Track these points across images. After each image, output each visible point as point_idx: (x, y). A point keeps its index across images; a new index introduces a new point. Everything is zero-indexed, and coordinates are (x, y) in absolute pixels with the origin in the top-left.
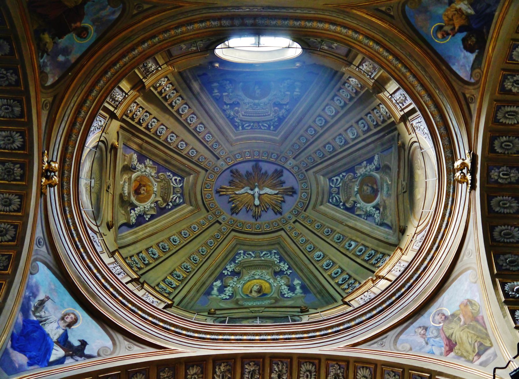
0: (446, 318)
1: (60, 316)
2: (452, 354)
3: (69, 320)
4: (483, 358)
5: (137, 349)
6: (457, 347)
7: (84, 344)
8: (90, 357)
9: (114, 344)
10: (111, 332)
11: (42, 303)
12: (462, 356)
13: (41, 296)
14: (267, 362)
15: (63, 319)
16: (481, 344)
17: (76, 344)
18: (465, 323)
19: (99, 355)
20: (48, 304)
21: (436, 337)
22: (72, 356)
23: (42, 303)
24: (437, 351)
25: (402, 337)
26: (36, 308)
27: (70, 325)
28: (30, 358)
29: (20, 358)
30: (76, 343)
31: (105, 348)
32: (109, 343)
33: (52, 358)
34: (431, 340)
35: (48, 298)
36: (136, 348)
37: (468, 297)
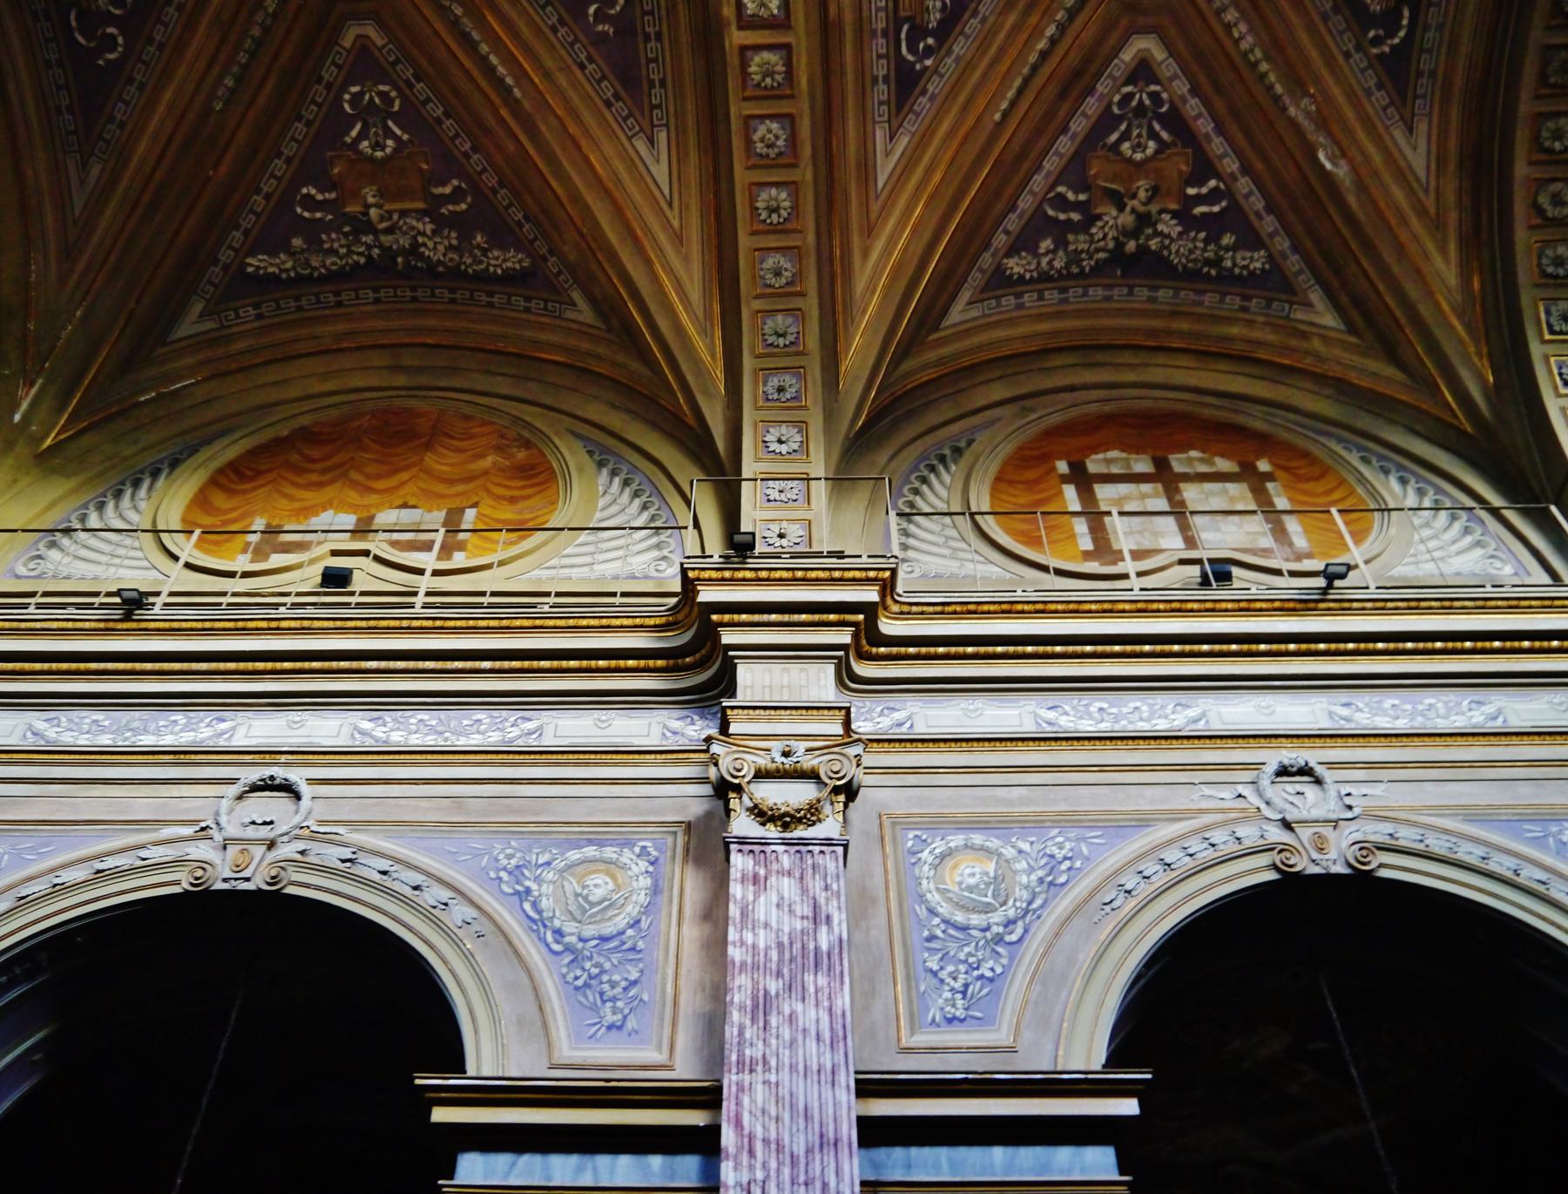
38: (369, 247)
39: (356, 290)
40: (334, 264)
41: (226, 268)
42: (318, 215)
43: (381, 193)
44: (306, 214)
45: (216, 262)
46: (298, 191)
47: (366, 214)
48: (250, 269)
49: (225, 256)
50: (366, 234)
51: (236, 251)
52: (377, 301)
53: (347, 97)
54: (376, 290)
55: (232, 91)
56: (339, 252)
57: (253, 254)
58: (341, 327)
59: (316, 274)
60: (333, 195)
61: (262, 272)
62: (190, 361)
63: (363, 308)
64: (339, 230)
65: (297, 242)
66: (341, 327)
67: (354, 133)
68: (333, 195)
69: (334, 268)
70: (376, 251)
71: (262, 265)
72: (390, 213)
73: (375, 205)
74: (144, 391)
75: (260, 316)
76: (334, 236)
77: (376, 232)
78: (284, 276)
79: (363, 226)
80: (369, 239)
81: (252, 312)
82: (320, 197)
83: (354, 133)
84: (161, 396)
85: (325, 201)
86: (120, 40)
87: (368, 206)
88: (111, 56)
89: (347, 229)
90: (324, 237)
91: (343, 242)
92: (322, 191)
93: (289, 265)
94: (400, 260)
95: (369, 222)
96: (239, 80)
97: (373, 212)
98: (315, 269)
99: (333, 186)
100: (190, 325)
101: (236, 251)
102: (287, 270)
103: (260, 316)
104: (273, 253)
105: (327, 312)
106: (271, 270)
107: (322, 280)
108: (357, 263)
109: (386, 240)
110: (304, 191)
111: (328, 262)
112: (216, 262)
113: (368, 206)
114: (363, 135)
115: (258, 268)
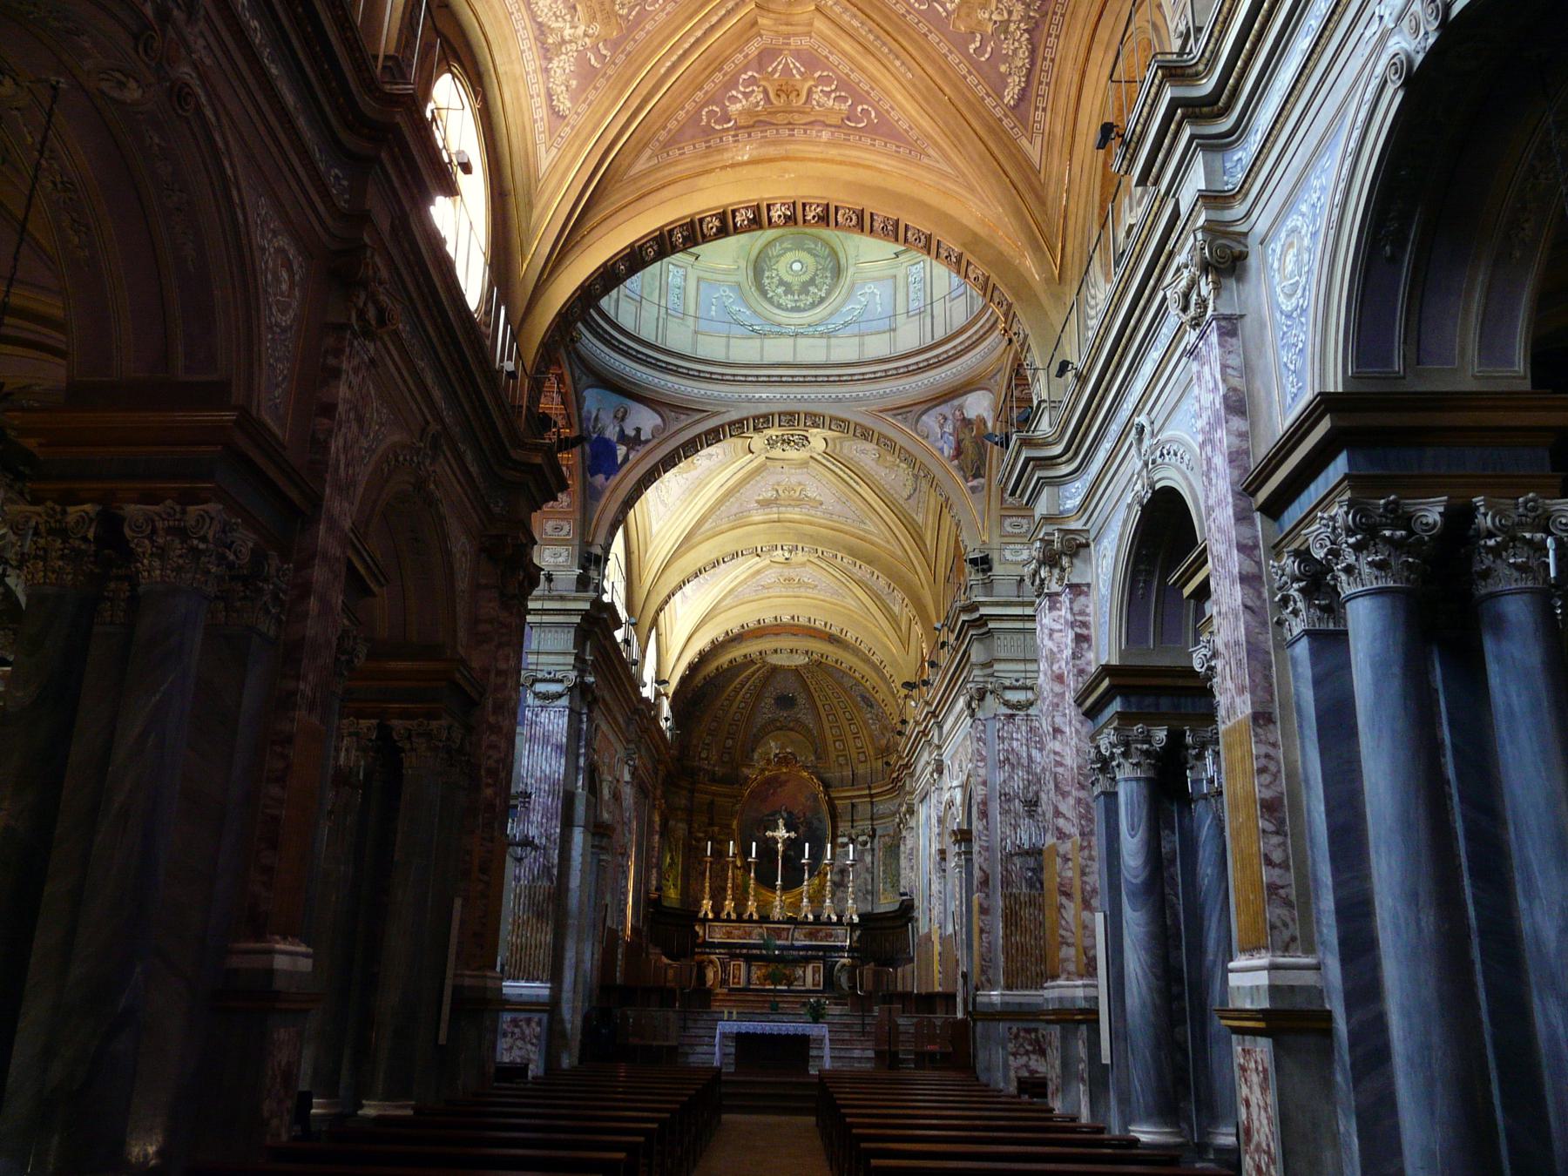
0: (964, 418)
1: (612, 416)
2: (956, 462)
3: (620, 415)
4: (975, 483)
5: (685, 420)
6: (962, 456)
7: (638, 430)
8: (647, 441)
9: (663, 420)
10: (658, 408)
11: (597, 418)
12: (962, 469)
13: (594, 416)
14: (803, 416)
15: (615, 417)
16: (978, 468)
17: (631, 433)
18: (975, 437)
19: (653, 437)
20: (602, 415)
21: (950, 434)
22: (633, 448)
23: (597, 418)
24: (946, 454)
25: (924, 418)
26: (594, 428)
27: (623, 419)
28: (605, 473)
29: (600, 478)
30: (632, 433)
31: (656, 428)
32: (659, 421)
33: (620, 460)
34: (946, 435)
35: (599, 410)
36: (683, 417)
37: (985, 415)
38: (1018, 28)
39: (1046, 47)
40: (1024, 53)
41: (1006, 115)
42: (989, 49)
43: (984, 7)
44: (987, 56)
45: (1000, 120)
46: (971, 55)
47: (995, 22)
48: (1012, 103)
49: (999, 113)
50: (1008, 27)
51: (998, 105)
52: (1058, 37)
53: (916, 5)
54: (1049, 35)
55: (903, 63)
56: (1017, 46)
57: (1002, 98)
58: (1070, 64)
59: (1028, 66)
60: (978, 36)
61: (1016, 97)
62: (1056, 162)
63: (1060, 47)
64: (1002, 42)
65: (1003, 68)
66: (1070, 64)
67: (941, 10)
68: (978, 36)
69: (1027, 54)
70: (1022, 25)
71: (1011, 94)
72: (997, 9)
73: (992, 13)
74: (1061, 197)
75: (1044, 110)
76: (1005, 46)
77: (1009, 21)
78: (1023, 85)
79: (1003, 27)
80: (1012, 27)
81: (1039, 113)
82: (978, 44)
83: (941, 10)
84: (1068, 191)
85: (981, 41)
86: (865, 107)
87: (990, 19)
88: (873, 115)
89: (1002, 37)
90: (1004, 52)
91: (1011, 41)
92: (974, 41)
93: (1017, 79)
94: (1032, 14)
95: (1001, 22)
96: (897, 57)
97: (995, 17)
98: (1024, 65)
99: (973, 33)
100: (1034, 151)
101: (998, 105)
102: (1020, 81)
103: (1044, 110)
104: (1006, 85)
105: (1055, 69)
106: (1016, 91)
107: (1033, 63)
108: (1028, 39)
109: (1015, 17)
110: (971, 51)
111: (1021, 56)
112: (1000, 120)
113: (990, 19)
114: (943, 6)
115: (1012, 97)
